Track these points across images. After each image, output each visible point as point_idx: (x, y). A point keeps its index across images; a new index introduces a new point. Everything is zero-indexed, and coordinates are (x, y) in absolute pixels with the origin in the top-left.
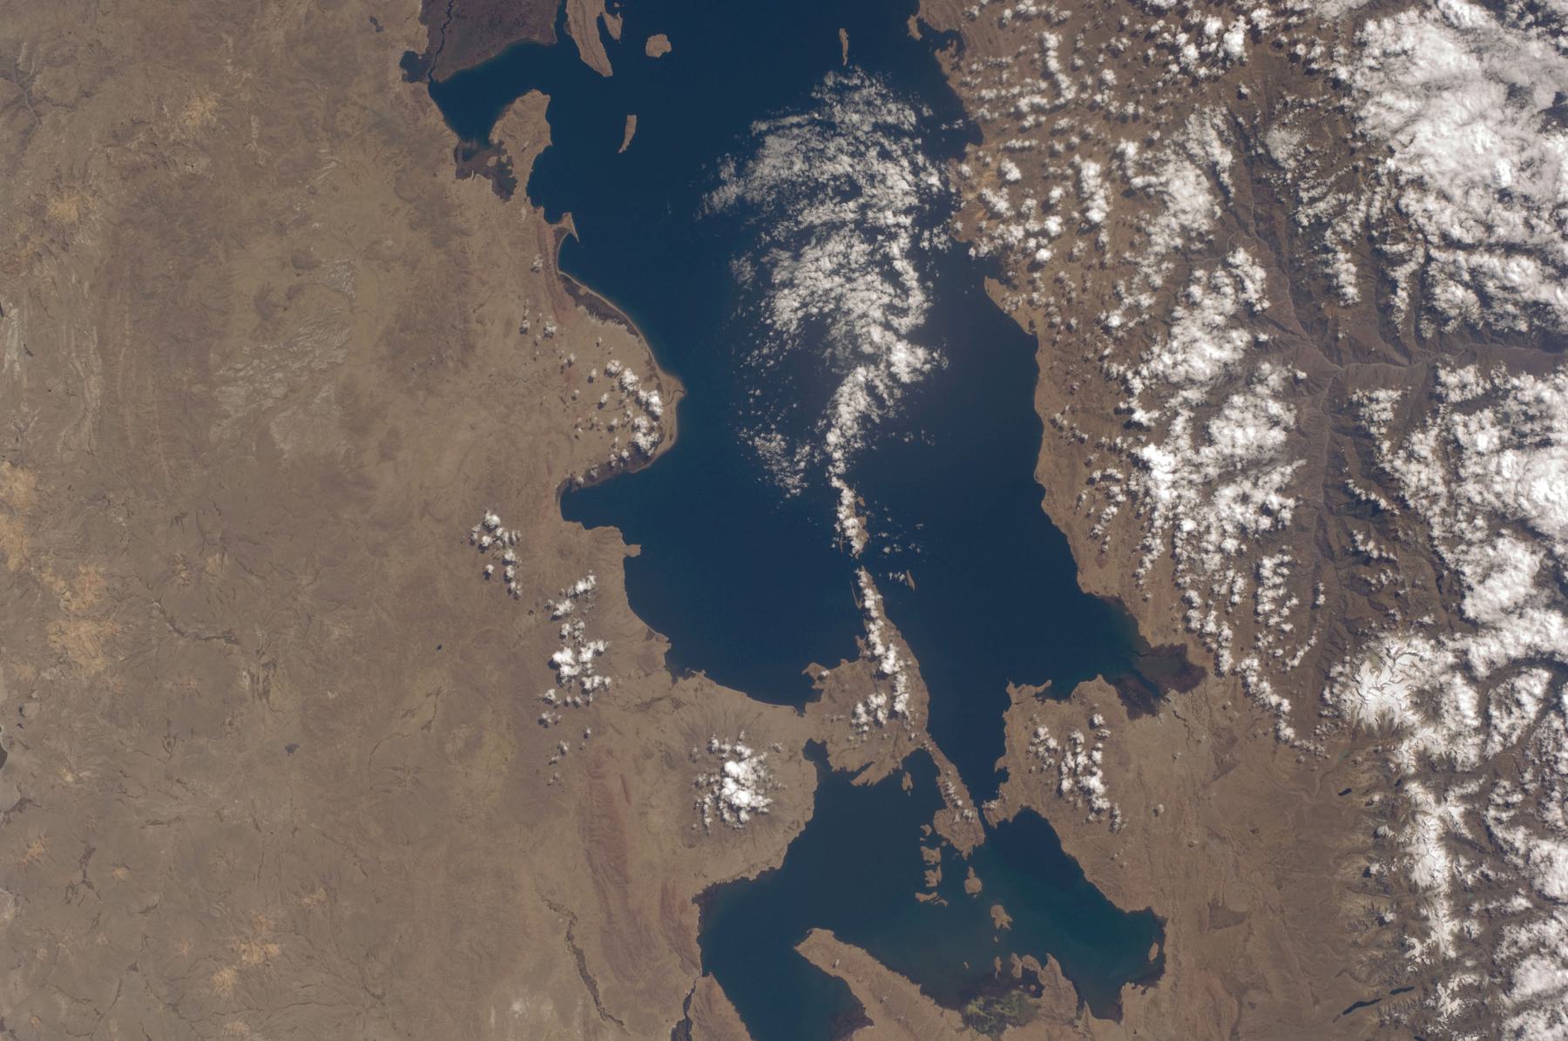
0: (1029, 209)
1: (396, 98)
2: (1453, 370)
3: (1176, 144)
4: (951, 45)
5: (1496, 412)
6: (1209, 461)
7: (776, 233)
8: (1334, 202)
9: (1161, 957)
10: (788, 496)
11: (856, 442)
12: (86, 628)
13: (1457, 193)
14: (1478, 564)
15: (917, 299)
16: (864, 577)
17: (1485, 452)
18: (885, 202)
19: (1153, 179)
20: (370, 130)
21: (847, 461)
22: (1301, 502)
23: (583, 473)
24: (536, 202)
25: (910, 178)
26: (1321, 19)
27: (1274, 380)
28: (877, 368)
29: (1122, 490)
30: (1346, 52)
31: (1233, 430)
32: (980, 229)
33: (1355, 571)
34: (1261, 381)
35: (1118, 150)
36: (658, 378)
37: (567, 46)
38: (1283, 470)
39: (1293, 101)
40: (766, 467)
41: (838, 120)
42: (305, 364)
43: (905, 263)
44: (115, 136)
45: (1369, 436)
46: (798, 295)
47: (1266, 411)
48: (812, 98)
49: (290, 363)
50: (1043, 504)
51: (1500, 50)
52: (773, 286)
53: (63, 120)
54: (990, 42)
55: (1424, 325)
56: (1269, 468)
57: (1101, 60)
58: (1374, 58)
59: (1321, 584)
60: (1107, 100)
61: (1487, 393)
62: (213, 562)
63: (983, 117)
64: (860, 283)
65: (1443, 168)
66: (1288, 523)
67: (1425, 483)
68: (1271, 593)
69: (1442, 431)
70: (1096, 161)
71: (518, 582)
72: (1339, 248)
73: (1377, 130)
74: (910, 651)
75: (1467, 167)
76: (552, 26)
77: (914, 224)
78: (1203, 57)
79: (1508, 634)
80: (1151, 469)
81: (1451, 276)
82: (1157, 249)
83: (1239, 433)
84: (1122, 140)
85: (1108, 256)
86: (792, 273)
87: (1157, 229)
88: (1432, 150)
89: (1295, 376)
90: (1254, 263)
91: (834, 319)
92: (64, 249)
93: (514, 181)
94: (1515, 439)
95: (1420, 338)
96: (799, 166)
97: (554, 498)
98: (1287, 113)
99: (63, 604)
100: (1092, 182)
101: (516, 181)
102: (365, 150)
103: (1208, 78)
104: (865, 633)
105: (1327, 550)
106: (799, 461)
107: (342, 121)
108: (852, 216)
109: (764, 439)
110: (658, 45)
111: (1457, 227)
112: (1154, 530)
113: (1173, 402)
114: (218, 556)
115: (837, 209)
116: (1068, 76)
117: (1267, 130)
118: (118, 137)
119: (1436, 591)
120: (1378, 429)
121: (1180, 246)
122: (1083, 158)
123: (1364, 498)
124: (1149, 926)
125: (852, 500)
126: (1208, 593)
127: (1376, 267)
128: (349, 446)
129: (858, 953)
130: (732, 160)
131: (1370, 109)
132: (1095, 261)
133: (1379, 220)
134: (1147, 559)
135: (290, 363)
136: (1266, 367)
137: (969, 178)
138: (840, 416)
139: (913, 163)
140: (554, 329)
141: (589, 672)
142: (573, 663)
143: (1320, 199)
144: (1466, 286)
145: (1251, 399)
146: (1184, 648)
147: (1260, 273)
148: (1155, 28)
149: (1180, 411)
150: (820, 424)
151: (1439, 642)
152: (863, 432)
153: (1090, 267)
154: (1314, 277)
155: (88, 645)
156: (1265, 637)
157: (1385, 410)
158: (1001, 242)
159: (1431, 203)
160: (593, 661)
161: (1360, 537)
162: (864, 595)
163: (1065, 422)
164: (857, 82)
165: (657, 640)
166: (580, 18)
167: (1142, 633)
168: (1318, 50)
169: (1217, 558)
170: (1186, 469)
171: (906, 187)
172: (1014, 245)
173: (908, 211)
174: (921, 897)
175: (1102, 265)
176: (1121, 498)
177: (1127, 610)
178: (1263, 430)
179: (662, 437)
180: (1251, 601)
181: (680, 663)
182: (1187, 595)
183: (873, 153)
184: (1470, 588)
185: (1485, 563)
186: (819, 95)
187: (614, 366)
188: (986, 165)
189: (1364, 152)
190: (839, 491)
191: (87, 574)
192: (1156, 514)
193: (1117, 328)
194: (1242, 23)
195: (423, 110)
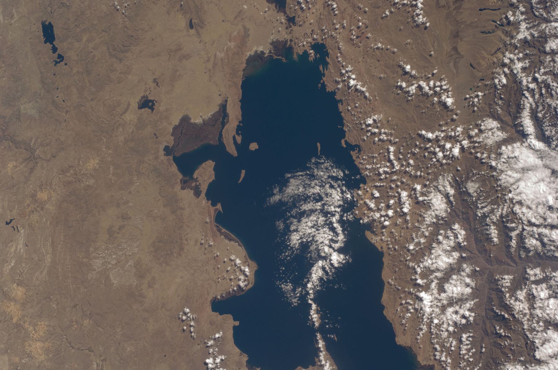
0: (382, 207)
1: (161, 161)
2: (532, 269)
3: (434, 186)
4: (356, 150)
5: (547, 285)
6: (444, 298)
7: (292, 213)
8: (490, 208)
10: (293, 306)
11: (318, 287)
12: (39, 344)
13: (534, 207)
14: (540, 339)
15: (341, 237)
16: (319, 336)
17: (543, 299)
18: (331, 203)
19: (426, 198)
20: (151, 172)
21: (314, 294)
22: (477, 315)
23: (220, 295)
24: (208, 199)
25: (340, 195)
26: (486, 145)
27: (468, 270)
28: (326, 261)
29: (412, 308)
30: (495, 156)
31: (453, 288)
32: (364, 214)
33: (496, 340)
34: (463, 271)
35: (414, 188)
36: (248, 262)
37: (222, 146)
38: (470, 302)
39: (476, 173)
40: (285, 295)
41: (316, 174)
42: (124, 253)
43: (337, 224)
44: (63, 171)
45: (502, 291)
46: (299, 235)
47: (465, 281)
48: (307, 166)
49: (118, 252)
50: (384, 312)
51: (549, 158)
52: (290, 231)
53: (45, 165)
54: (370, 149)
55: (522, 253)
56: (465, 302)
57: (409, 156)
58: (505, 159)
59: (483, 344)
60: (410, 170)
61: (544, 278)
62: (86, 322)
63: (367, 174)
64: (321, 231)
65: (529, 198)
66: (472, 322)
67: (522, 309)
68: (465, 347)
69: (528, 290)
70: (406, 191)
71: (195, 333)
72: (491, 224)
73: (505, 184)
74: (334, 363)
75: (537, 198)
76: (217, 139)
77: (341, 211)
78: (445, 156)
79: (551, 365)
80: (423, 301)
81: (531, 236)
82: (427, 222)
83: (455, 289)
84: (415, 184)
85: (410, 224)
86: (297, 227)
87: (427, 216)
88: (525, 191)
89: (475, 269)
90: (461, 229)
91: (312, 244)
92: (42, 209)
93: (201, 191)
94: (554, 294)
95: (520, 257)
96: (301, 189)
97: (209, 304)
98: (474, 177)
99: (31, 335)
100: (404, 198)
101: (202, 191)
102: (149, 179)
103: (446, 164)
104: (318, 356)
105: (486, 332)
106: (297, 293)
107: (142, 168)
108: (319, 207)
109: (285, 285)
110: (254, 146)
111: (533, 218)
112: (423, 323)
113: (431, 277)
114: (88, 320)
115: (314, 205)
116: (397, 161)
117: (466, 183)
118: (64, 171)
119: (525, 348)
120: (505, 289)
121: (435, 222)
122: (402, 190)
123: (499, 313)
125: (315, 308)
126: (442, 346)
127: (505, 232)
128: (137, 282)
130: (278, 187)
131: (503, 176)
132: (405, 226)
133: (506, 215)
134: (421, 333)
135: (118, 252)
136: (465, 266)
137: (361, 196)
138: (312, 278)
139: (342, 190)
140: (212, 243)
141: (219, 367)
142: (213, 363)
143: (485, 207)
144: (537, 239)
145: (459, 277)
146: (433, 366)
147: (463, 232)
148: (428, 146)
149: (434, 280)
150: (305, 280)
151: (526, 367)
152: (320, 284)
153: (403, 228)
154: (483, 234)
155: (39, 351)
156: (463, 363)
157: (507, 282)
158: (371, 218)
159: (524, 210)
160: (220, 363)
161: (498, 328)
162: (319, 342)
163: (393, 283)
164: (323, 161)
165: (243, 356)
166: (227, 136)
167: (418, 360)
168: (485, 155)
169: (446, 333)
170: (435, 301)
171: (339, 198)
172: (376, 220)
173: (339, 206)
175: (407, 228)
176: (412, 311)
177: (414, 351)
178: (464, 288)
179: (249, 283)
180: (458, 350)
182: (435, 346)
183: (328, 186)
184: (538, 348)
185: (543, 339)
186: (309, 165)
187: (233, 257)
188: (367, 191)
189: (500, 191)
190: (311, 305)
191: (41, 325)
192: (425, 317)
193: (412, 250)
194: (458, 145)
195: (171, 167)
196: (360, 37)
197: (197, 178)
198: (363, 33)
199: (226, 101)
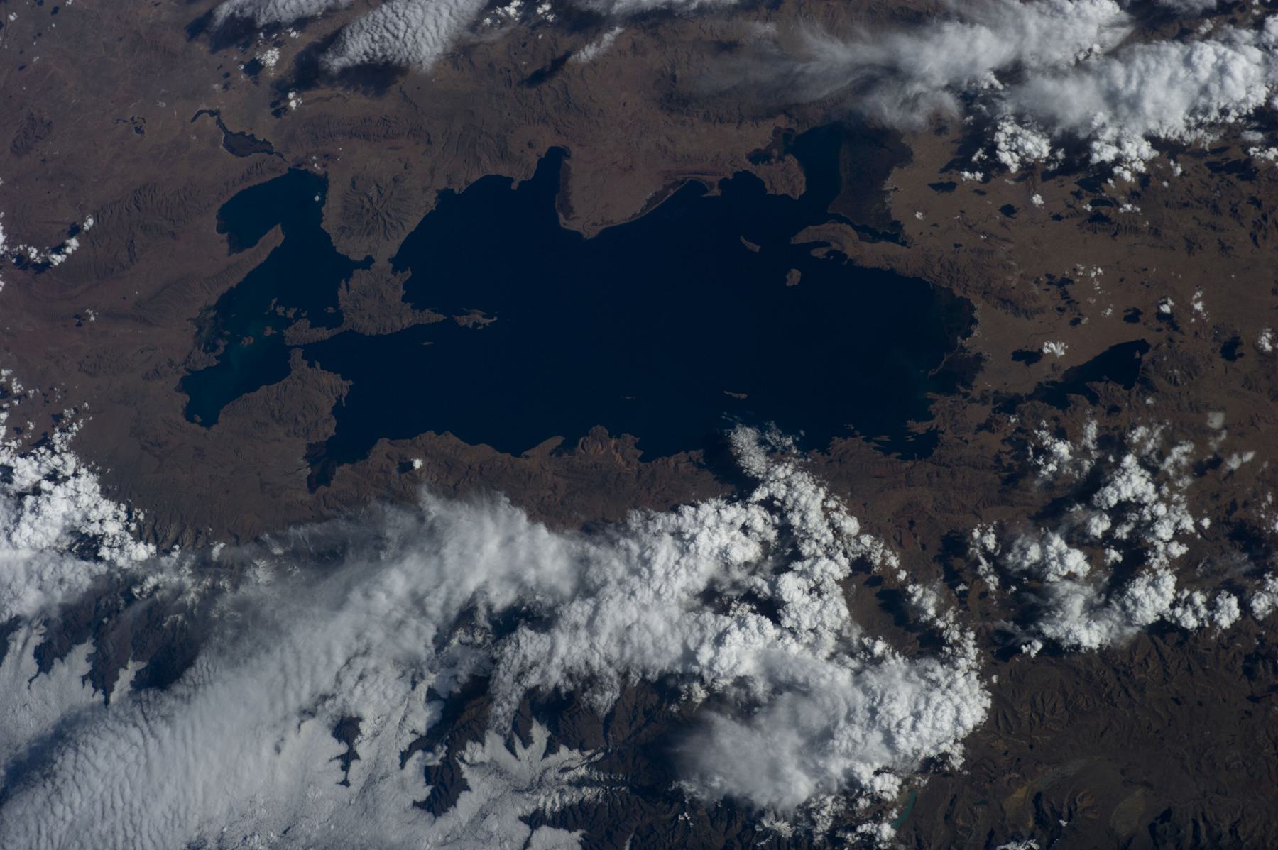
9: (193, 421)
16: (441, 317)
24: (736, 174)
93: (756, 164)
110: (794, 277)
124: (209, 422)
129: (264, 257)
146: (328, 485)
167: (345, 465)
174: (274, 301)
181: (445, 197)
196: (910, 529)
197: (783, 161)
198: (915, 536)
199: (904, 244)
